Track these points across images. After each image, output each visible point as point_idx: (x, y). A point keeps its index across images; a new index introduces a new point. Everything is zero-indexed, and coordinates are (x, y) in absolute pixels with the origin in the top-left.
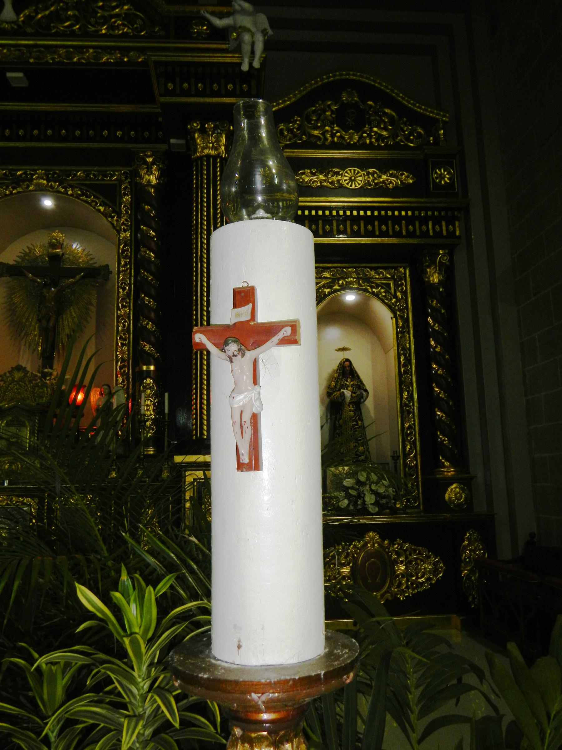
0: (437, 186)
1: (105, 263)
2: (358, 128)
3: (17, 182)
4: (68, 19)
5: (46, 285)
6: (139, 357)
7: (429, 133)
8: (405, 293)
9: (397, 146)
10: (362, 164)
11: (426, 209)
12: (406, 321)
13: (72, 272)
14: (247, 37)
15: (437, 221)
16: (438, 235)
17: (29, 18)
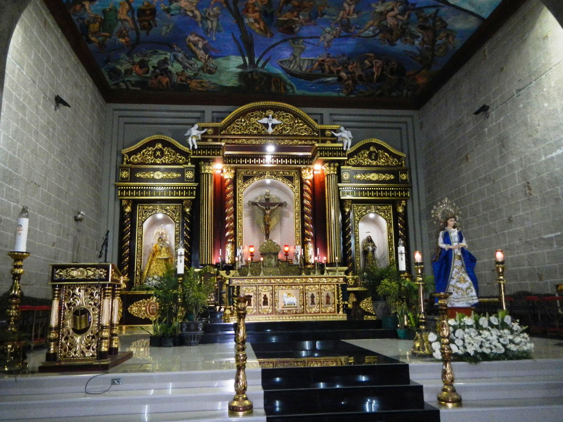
0: (402, 180)
1: (284, 201)
2: (376, 160)
3: (261, 175)
4: (288, 130)
5: (266, 209)
6: (304, 236)
7: (399, 161)
8: (390, 214)
9: (388, 166)
10: (377, 172)
11: (398, 188)
12: (391, 224)
13: (274, 204)
14: (346, 142)
15: (402, 191)
16: (402, 196)
17: (276, 130)
